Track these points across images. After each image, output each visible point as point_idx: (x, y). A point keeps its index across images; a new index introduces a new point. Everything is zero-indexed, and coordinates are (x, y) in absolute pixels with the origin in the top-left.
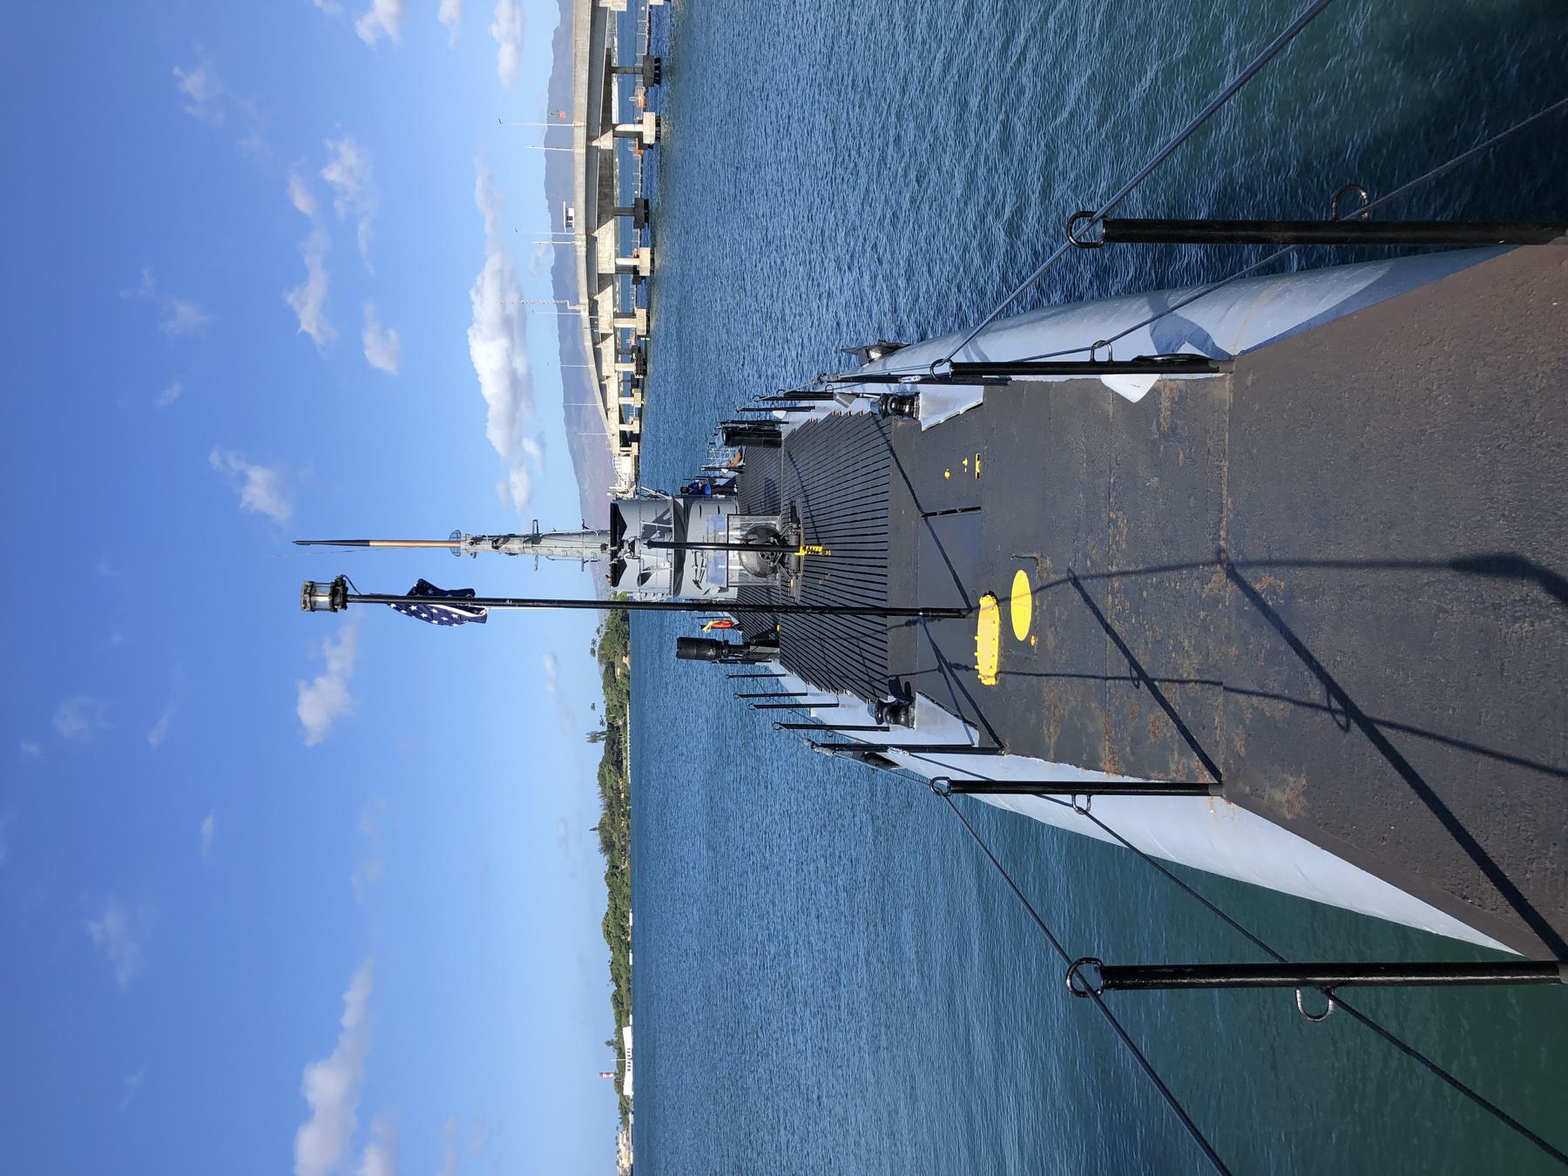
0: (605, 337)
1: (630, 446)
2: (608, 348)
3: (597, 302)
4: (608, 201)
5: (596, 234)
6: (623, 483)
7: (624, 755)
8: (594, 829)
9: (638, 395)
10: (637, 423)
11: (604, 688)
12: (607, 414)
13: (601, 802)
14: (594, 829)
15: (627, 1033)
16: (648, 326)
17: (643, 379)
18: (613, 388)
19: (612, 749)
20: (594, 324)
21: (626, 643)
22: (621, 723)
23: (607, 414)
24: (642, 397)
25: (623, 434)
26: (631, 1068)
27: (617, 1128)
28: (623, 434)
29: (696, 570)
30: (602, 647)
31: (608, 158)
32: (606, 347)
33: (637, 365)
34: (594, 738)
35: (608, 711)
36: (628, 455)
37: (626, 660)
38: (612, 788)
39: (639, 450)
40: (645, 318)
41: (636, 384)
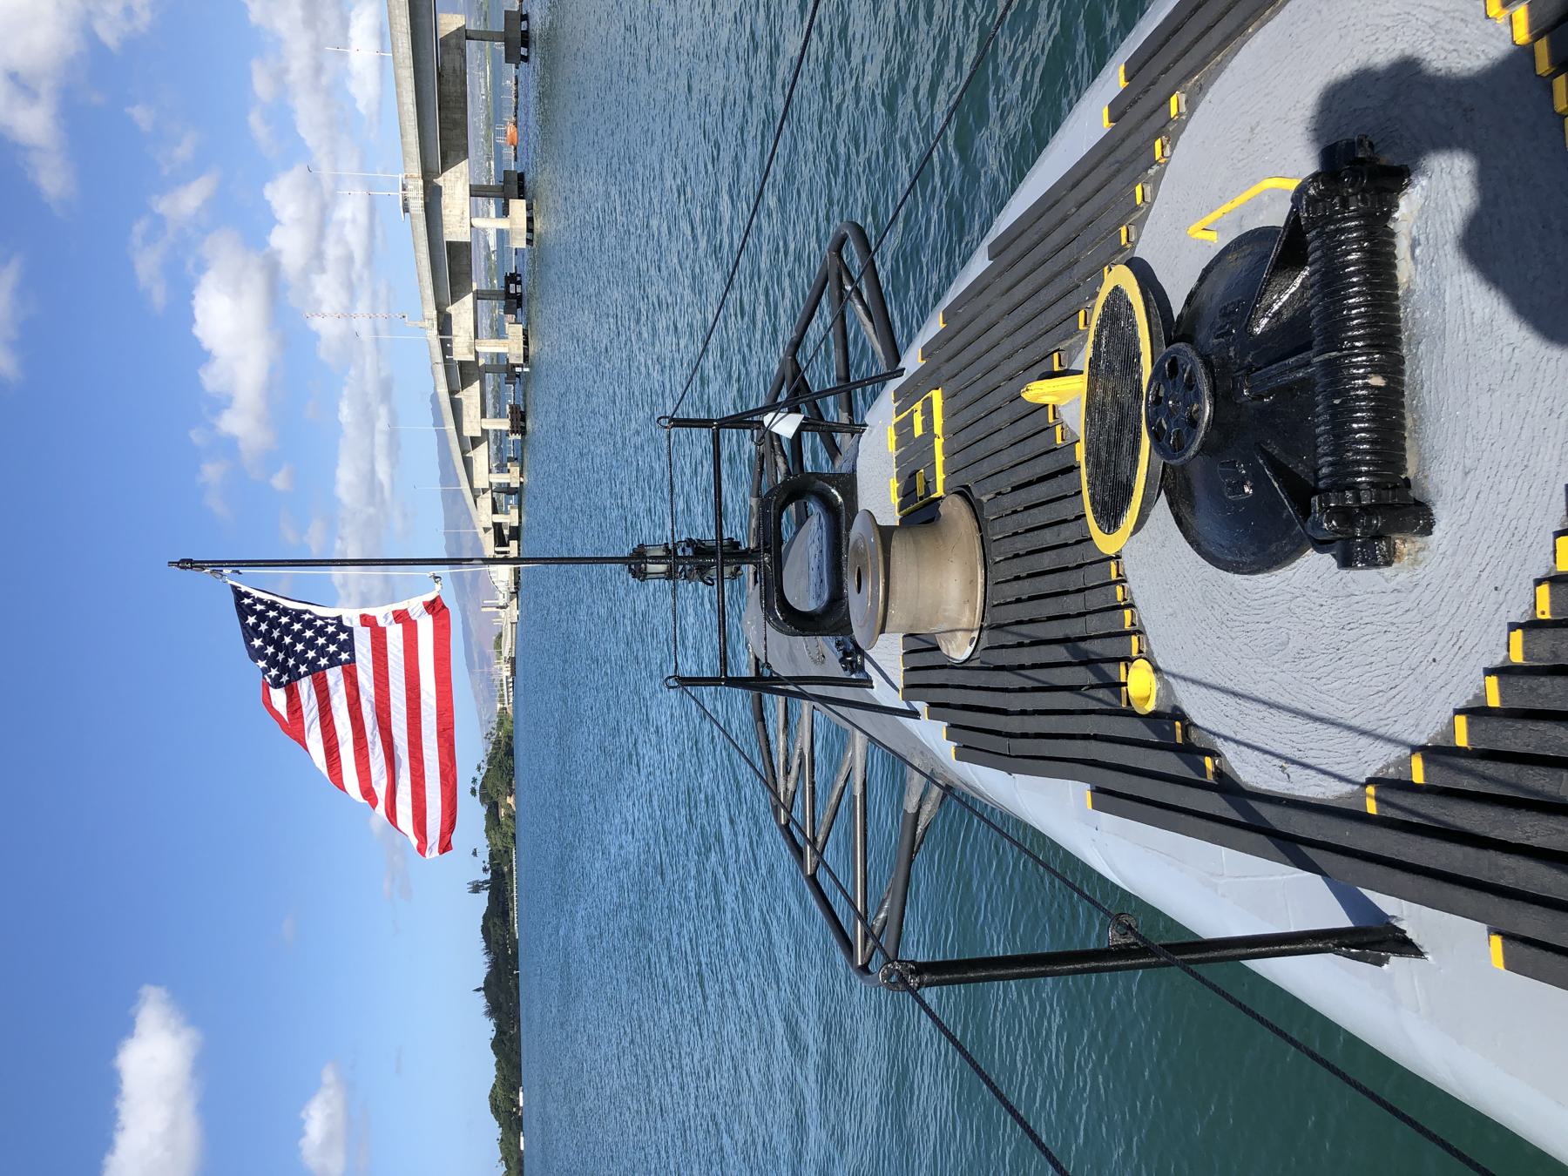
1: (508, 545)
3: (449, 316)
4: (458, 131)
5: (440, 181)
6: (501, 596)
7: (510, 905)
8: (478, 990)
9: (515, 470)
10: (515, 512)
11: (487, 831)
12: (475, 502)
13: (486, 959)
14: (478, 990)
16: (526, 350)
18: (481, 456)
19: (497, 898)
20: (446, 348)
21: (511, 780)
22: (506, 869)
23: (475, 502)
24: (521, 475)
25: (498, 527)
28: (498, 527)
30: (483, 786)
31: (457, 65)
32: (469, 397)
33: (512, 420)
34: (476, 888)
35: (491, 856)
37: (510, 800)
38: (497, 943)
39: (519, 549)
40: (522, 337)
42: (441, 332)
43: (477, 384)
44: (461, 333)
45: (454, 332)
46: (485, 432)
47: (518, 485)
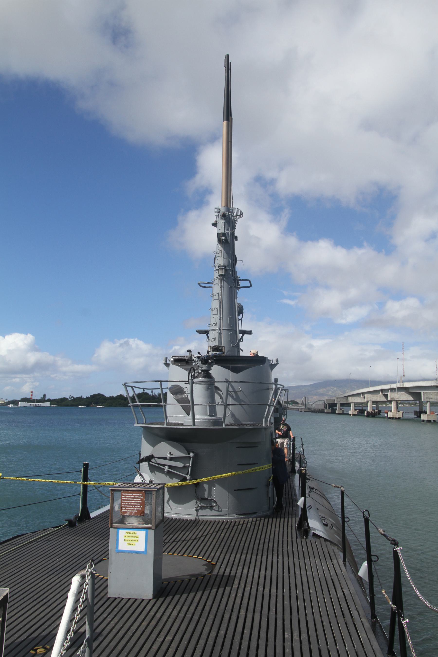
0: (386, 396)
2: (380, 397)
15: (48, 404)
17: (364, 416)
25: (335, 405)
26: (31, 406)
27: (7, 399)
28: (335, 405)
29: (165, 458)
32: (380, 396)
36: (324, 407)
41: (361, 412)
42: (398, 388)
43: (413, 399)
44: (398, 396)
45: (398, 393)
46: (368, 401)
47: (350, 413)
